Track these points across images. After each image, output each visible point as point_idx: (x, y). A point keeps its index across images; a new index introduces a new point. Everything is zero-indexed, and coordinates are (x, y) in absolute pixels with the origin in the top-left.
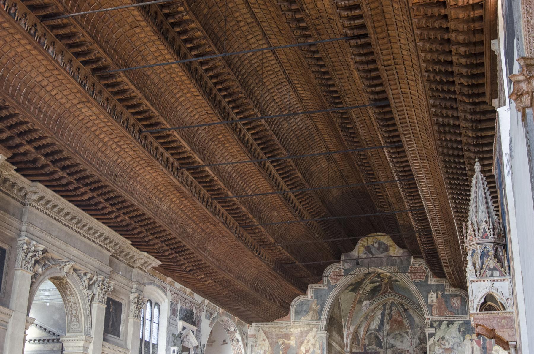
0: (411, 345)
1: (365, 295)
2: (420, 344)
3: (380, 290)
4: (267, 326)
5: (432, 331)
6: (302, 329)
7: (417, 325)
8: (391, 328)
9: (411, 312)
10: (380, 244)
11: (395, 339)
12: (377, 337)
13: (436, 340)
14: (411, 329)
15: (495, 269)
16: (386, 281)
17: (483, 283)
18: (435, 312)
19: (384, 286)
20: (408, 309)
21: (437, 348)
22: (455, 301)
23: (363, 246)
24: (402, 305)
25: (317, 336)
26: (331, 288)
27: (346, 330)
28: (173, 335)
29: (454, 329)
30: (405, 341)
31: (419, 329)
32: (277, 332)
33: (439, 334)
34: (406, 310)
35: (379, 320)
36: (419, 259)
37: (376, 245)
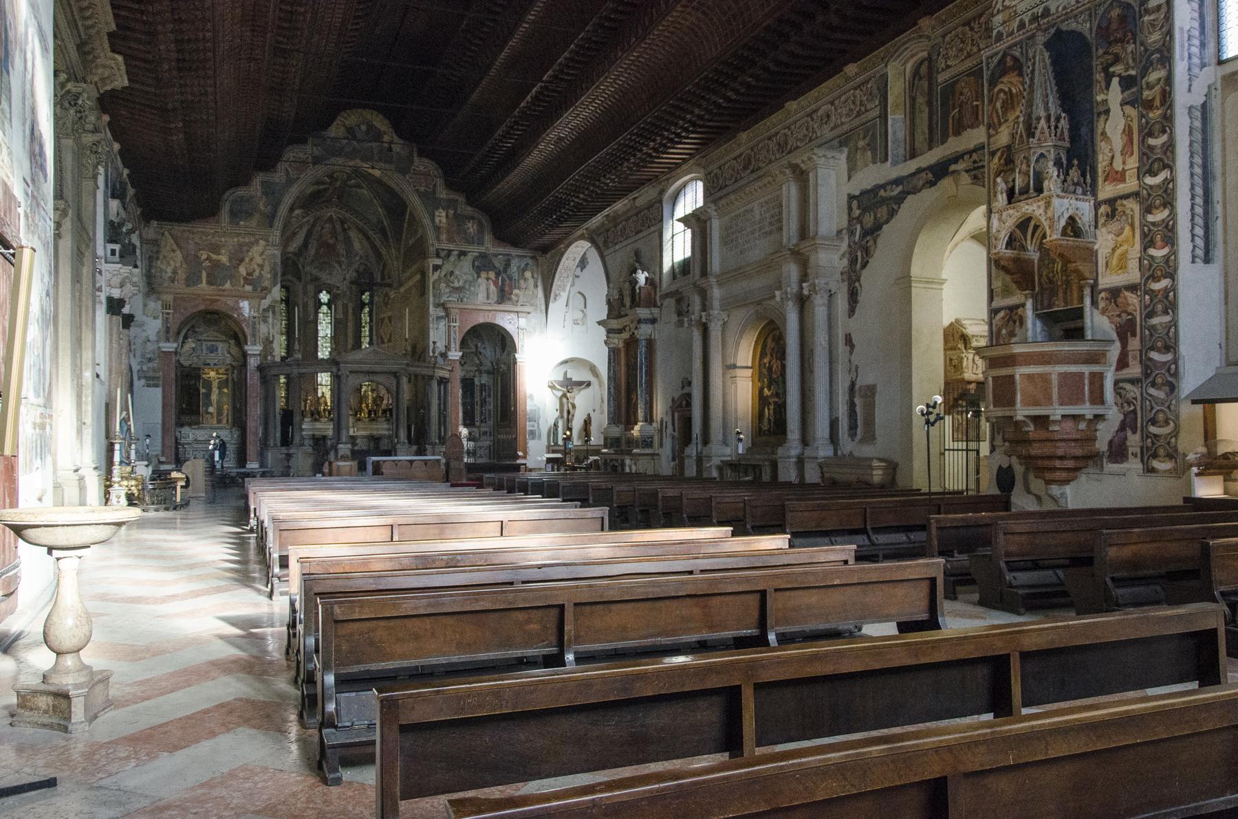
0: (345, 279)
4: (178, 229)
5: (438, 262)
6: (242, 240)
8: (317, 253)
9: (353, 234)
10: (371, 127)
13: (443, 273)
15: (1077, 184)
16: (338, 183)
17: (1066, 201)
18: (444, 237)
19: (330, 191)
20: (349, 228)
21: (443, 285)
22: (470, 225)
23: (344, 125)
24: (343, 222)
25: (266, 253)
26: (290, 182)
28: (112, 223)
29: (466, 264)
31: (357, 258)
32: (197, 240)
33: (447, 267)
34: (344, 230)
36: (426, 160)
37: (364, 128)
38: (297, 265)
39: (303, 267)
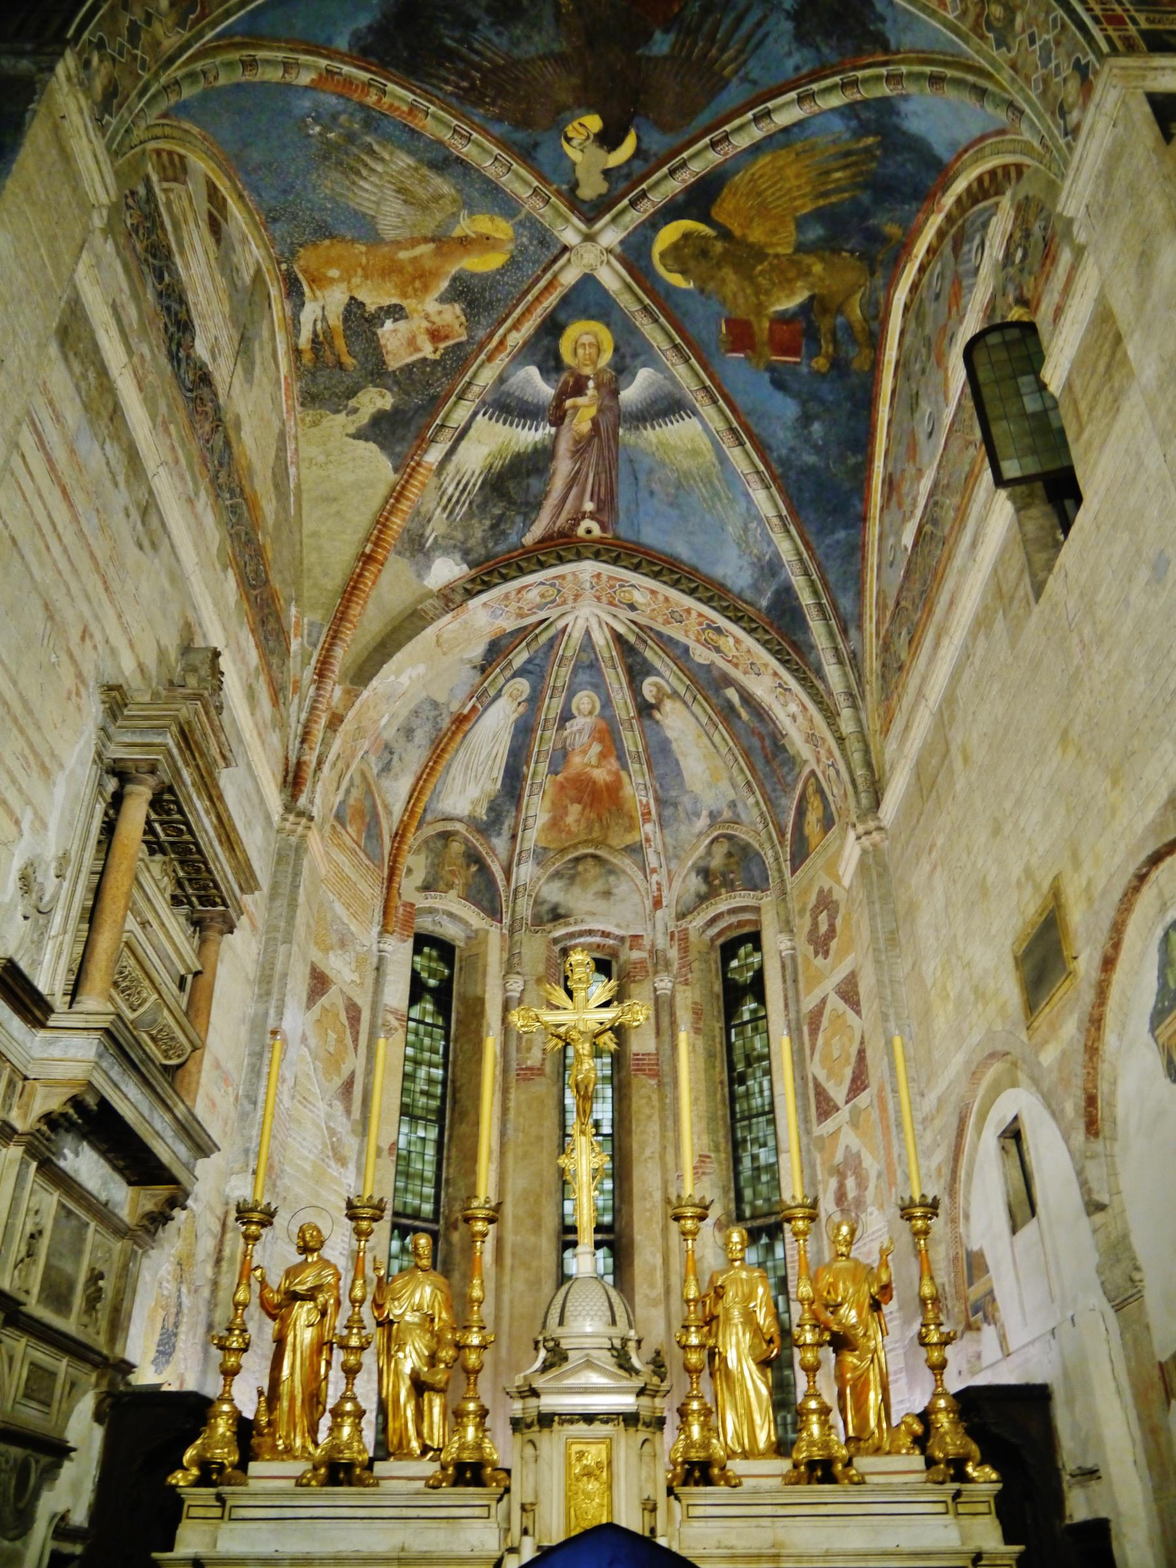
0: (657, 904)
1: (450, 507)
2: (702, 899)
3: (538, 506)
7: (696, 800)
8: (555, 823)
11: (572, 879)
12: (473, 858)
14: (662, 824)
19: (563, 467)
24: (637, 670)
27: (312, 691)
30: (622, 888)
31: (702, 823)
34: (646, 709)
35: (499, 773)
38: (484, 869)
39: (508, 872)
